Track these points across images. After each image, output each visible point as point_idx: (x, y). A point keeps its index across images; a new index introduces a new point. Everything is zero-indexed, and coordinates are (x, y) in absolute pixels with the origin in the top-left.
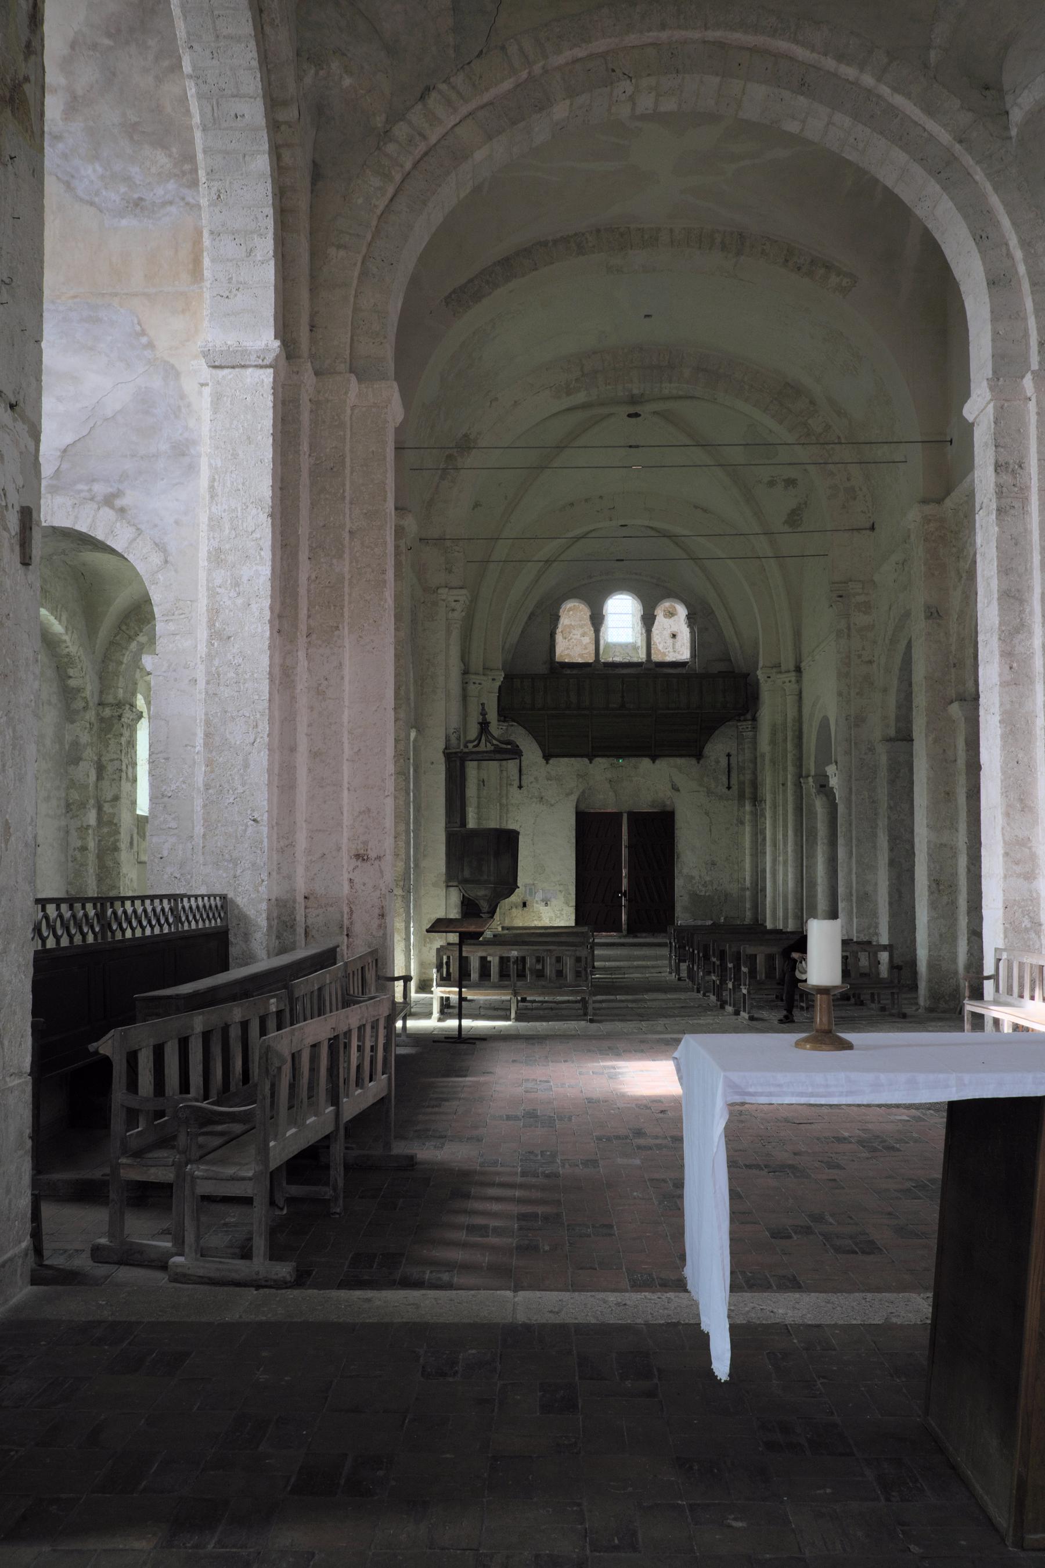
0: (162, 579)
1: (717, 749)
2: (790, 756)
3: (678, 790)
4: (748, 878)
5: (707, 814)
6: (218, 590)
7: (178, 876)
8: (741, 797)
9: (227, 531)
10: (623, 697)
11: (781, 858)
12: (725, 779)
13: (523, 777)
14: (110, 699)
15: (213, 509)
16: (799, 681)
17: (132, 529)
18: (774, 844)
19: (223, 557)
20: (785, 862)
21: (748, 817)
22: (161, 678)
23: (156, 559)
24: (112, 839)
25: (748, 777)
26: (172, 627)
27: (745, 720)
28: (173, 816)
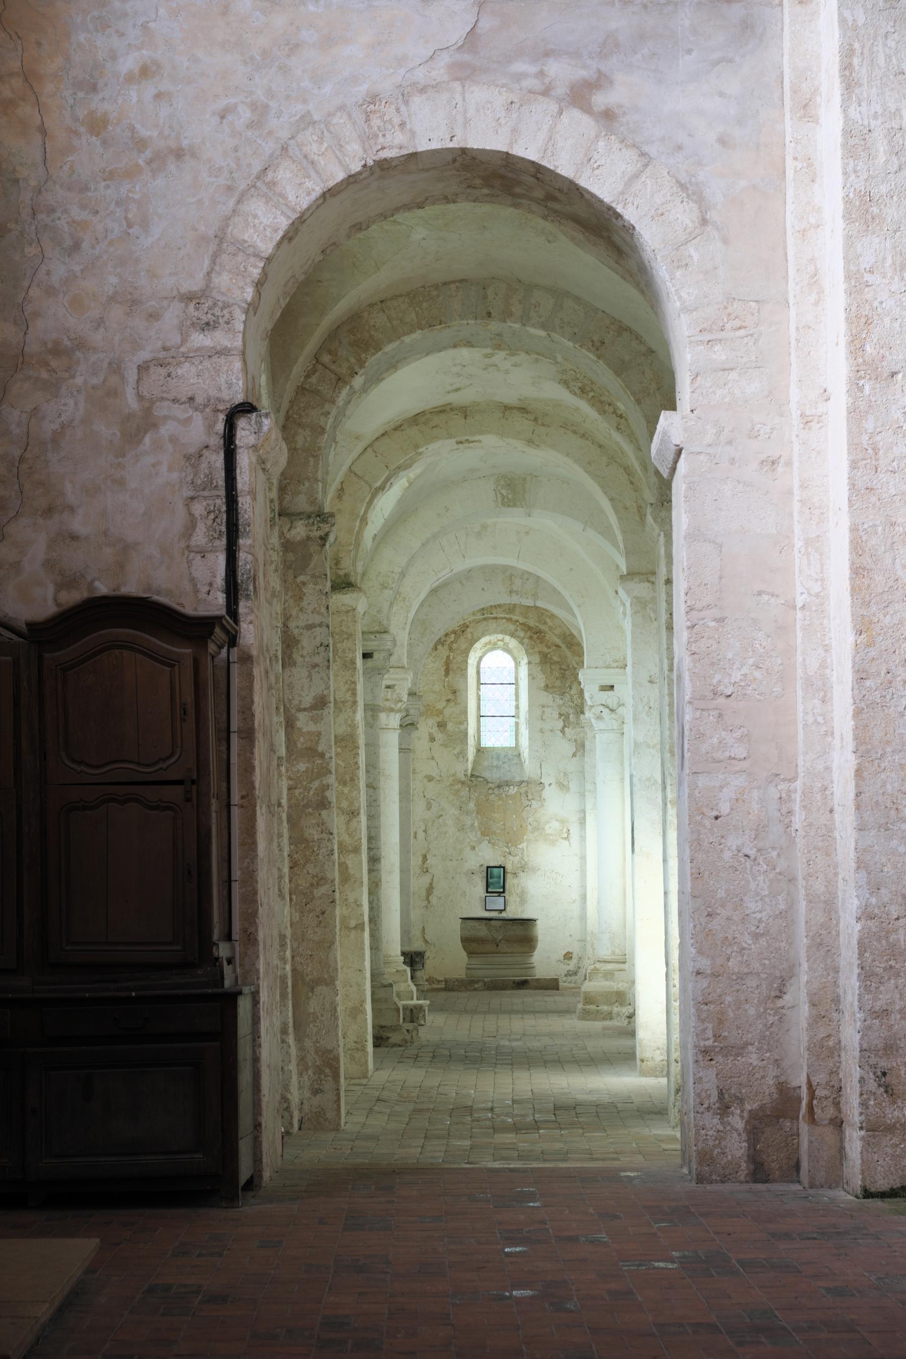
0: (696, 256)
6: (868, 277)
7: (752, 853)
9: (882, 158)
14: (301, 503)
15: (853, 112)
17: (631, 155)
19: (875, 210)
22: (702, 457)
23: (683, 215)
24: (316, 784)
26: (720, 354)
28: (738, 734)
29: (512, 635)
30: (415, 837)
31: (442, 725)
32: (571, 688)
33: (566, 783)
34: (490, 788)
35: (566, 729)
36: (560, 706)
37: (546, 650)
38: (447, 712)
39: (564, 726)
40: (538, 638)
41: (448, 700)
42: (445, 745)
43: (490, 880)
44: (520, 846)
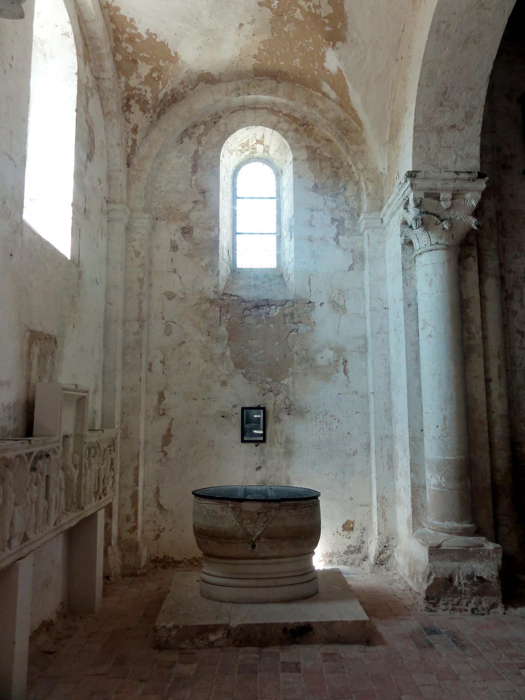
29: (274, 127)
30: (150, 370)
31: (186, 231)
32: (345, 189)
33: (341, 303)
34: (246, 309)
35: (340, 237)
36: (332, 210)
37: (314, 145)
38: (194, 216)
39: (338, 234)
40: (305, 131)
41: (195, 202)
42: (190, 256)
43: (247, 426)
44: (285, 382)
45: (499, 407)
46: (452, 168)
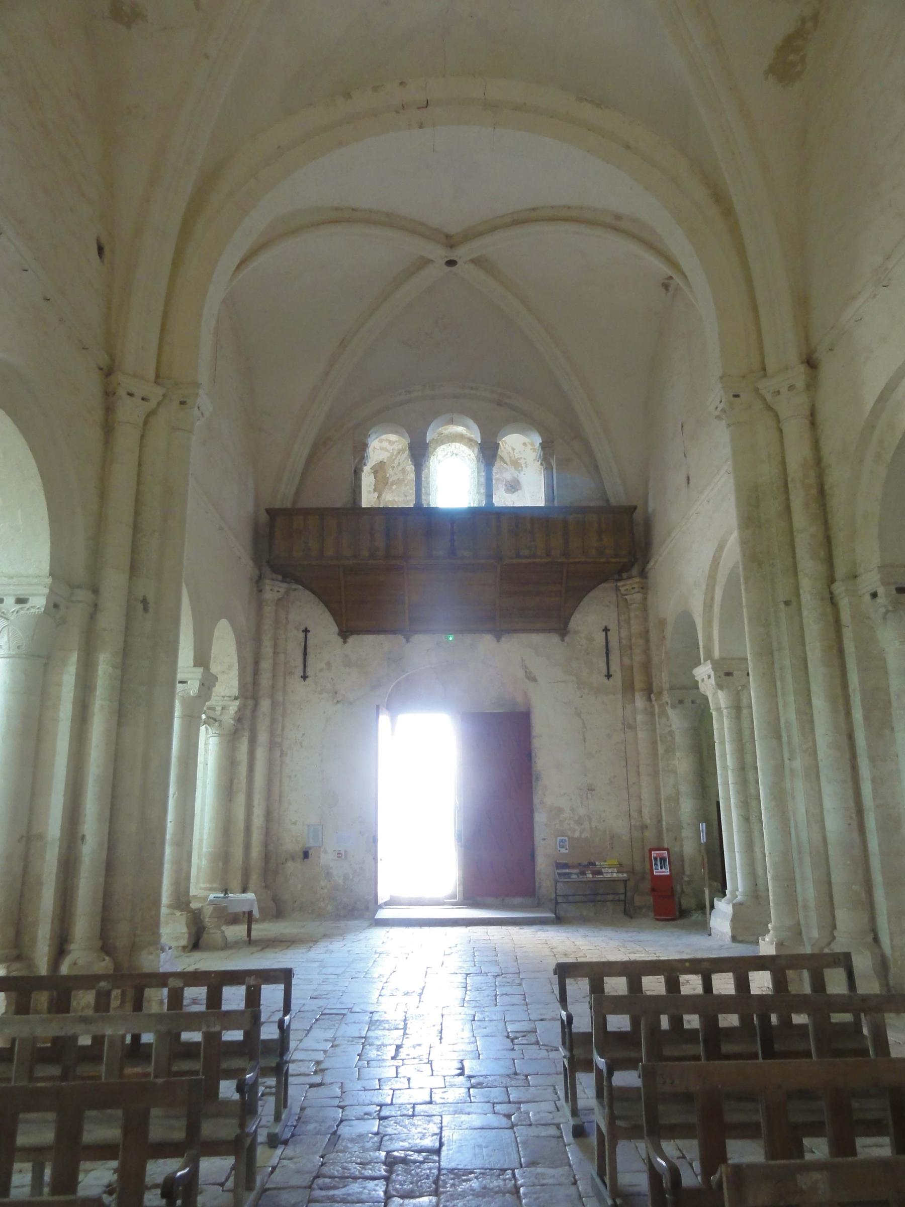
1: (593, 617)
2: (803, 542)
3: (534, 680)
4: (646, 811)
5: (579, 714)
8: (629, 687)
10: (452, 541)
11: (798, 764)
12: (602, 664)
13: (310, 662)
16: (812, 385)
18: (775, 731)
20: (813, 773)
21: (640, 718)
25: (638, 657)
27: (630, 578)
45: (258, 820)
46: (223, 694)
